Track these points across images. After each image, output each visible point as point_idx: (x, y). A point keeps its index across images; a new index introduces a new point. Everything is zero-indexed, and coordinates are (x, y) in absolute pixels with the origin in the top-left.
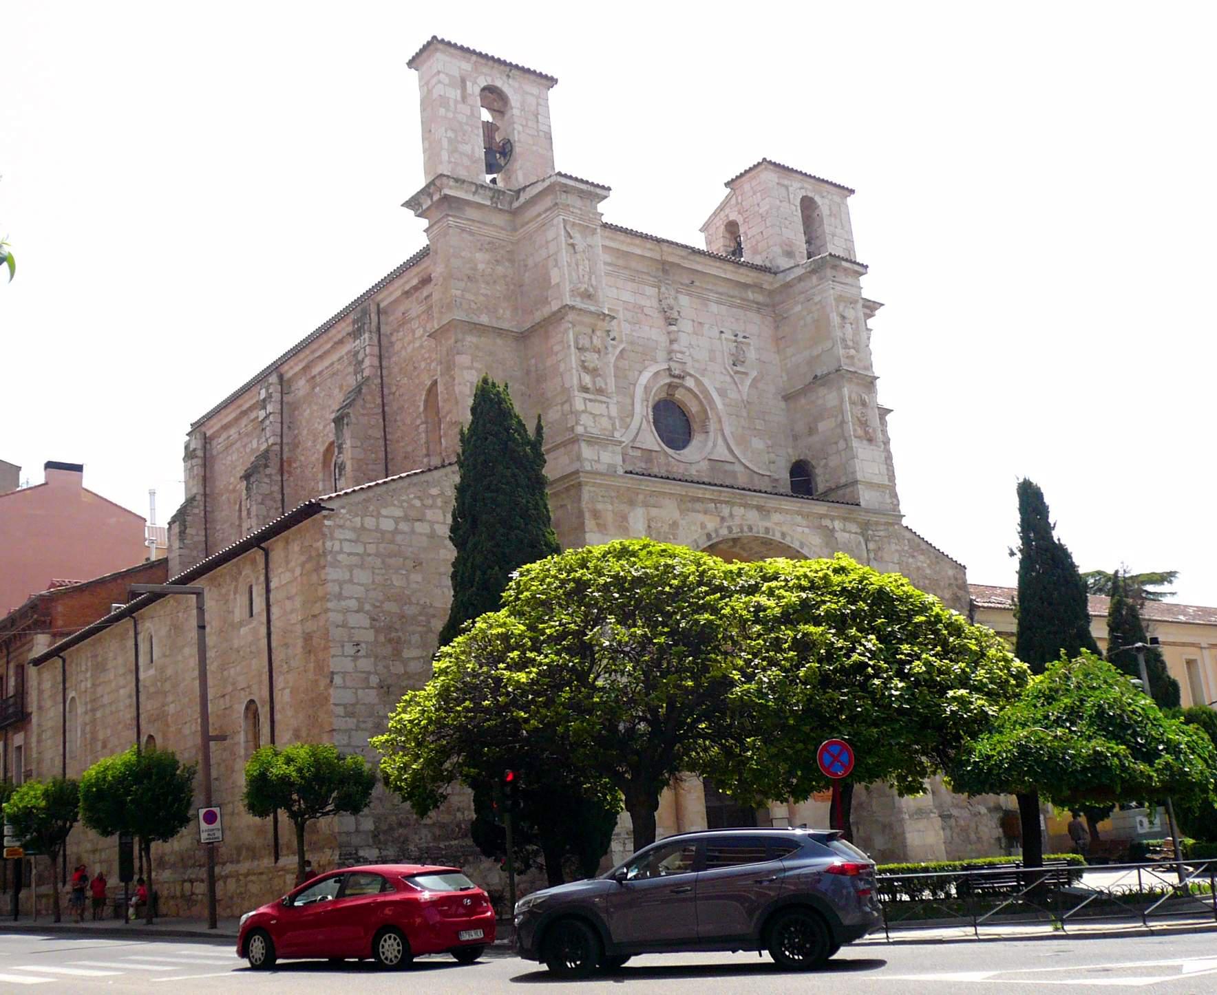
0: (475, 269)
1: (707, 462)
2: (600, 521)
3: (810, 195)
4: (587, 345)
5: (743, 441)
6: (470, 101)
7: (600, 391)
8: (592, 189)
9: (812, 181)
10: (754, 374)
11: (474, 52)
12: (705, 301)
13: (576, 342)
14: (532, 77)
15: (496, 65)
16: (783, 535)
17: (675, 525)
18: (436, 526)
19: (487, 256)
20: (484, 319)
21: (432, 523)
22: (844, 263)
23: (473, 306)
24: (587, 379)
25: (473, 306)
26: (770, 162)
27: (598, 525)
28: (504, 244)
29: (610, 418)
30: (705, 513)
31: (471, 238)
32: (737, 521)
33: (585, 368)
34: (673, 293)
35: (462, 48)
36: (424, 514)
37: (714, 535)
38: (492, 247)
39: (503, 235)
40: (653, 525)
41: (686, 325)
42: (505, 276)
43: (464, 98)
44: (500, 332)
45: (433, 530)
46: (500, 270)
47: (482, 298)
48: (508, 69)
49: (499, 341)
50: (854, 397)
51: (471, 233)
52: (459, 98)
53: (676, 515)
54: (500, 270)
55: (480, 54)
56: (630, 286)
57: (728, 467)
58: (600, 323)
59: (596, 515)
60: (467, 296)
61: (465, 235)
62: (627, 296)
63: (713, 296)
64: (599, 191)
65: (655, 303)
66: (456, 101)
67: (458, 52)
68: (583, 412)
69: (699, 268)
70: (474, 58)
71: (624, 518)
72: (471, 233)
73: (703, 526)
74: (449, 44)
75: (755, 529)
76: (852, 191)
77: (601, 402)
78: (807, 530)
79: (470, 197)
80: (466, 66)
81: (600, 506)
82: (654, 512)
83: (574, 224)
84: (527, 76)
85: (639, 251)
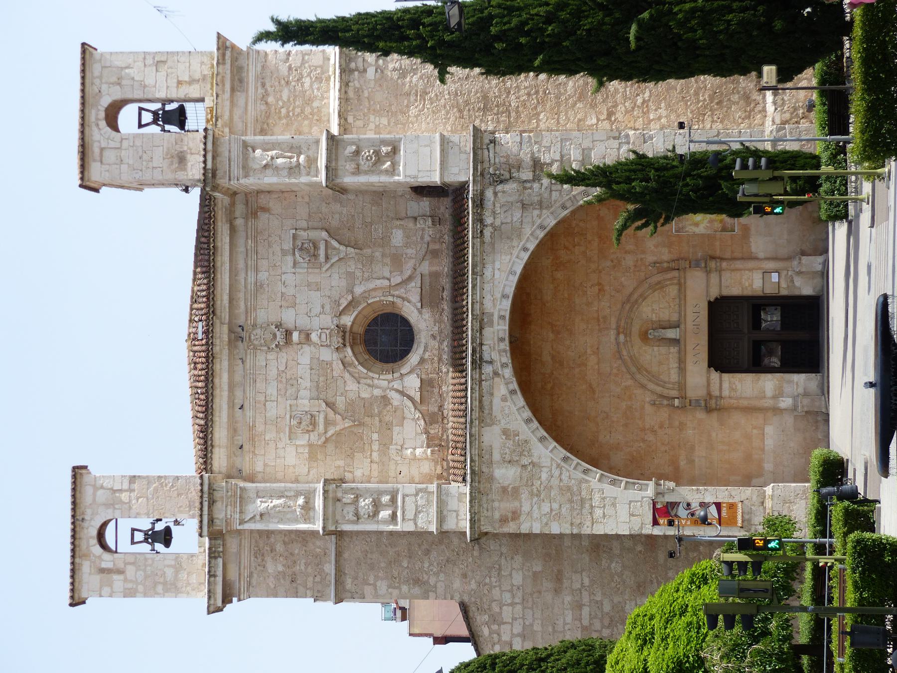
0: (283, 574)
1: (424, 310)
2: (510, 515)
3: (102, 115)
4: (351, 509)
5: (397, 261)
6: (121, 565)
7: (393, 500)
8: (206, 496)
9: (87, 111)
10: (324, 234)
11: (73, 563)
12: (259, 287)
13: (353, 522)
14: (78, 495)
15: (77, 536)
16: (504, 296)
17: (505, 432)
18: (515, 631)
19: (269, 560)
20: (330, 568)
21: (513, 635)
22: (209, 165)
23: (318, 579)
24: (385, 514)
25: (318, 579)
26: (82, 179)
27: (513, 519)
28: (253, 541)
29: (417, 495)
30: (492, 394)
31: (255, 575)
32: (495, 356)
33: (376, 513)
34: (258, 331)
35: (72, 577)
36: (506, 642)
37: (511, 387)
38: (259, 554)
39: (246, 543)
40: (508, 458)
41: (289, 318)
42: (285, 543)
43: (120, 572)
44: (339, 554)
45: (518, 635)
46: (279, 547)
47: (310, 570)
48: (77, 523)
49: (346, 555)
50: (350, 166)
51: (251, 575)
52: (121, 577)
53: (496, 429)
54: (279, 547)
55: (73, 557)
56: (260, 385)
57: (427, 280)
58: (331, 495)
59: (504, 520)
60: (310, 584)
61: (254, 582)
62: (272, 390)
63: (251, 279)
64: (206, 488)
65: (271, 356)
66: (125, 580)
67: (76, 577)
68: (416, 524)
69: (226, 298)
70: (77, 560)
71: (504, 490)
72: (251, 575)
73: (504, 399)
74: (72, 590)
75: (501, 335)
76: (83, 44)
77: (404, 502)
78: (497, 265)
79: (219, 579)
80: (86, 567)
81: (497, 515)
82: (496, 456)
83: (241, 512)
84: (78, 501)
85: (225, 376)
